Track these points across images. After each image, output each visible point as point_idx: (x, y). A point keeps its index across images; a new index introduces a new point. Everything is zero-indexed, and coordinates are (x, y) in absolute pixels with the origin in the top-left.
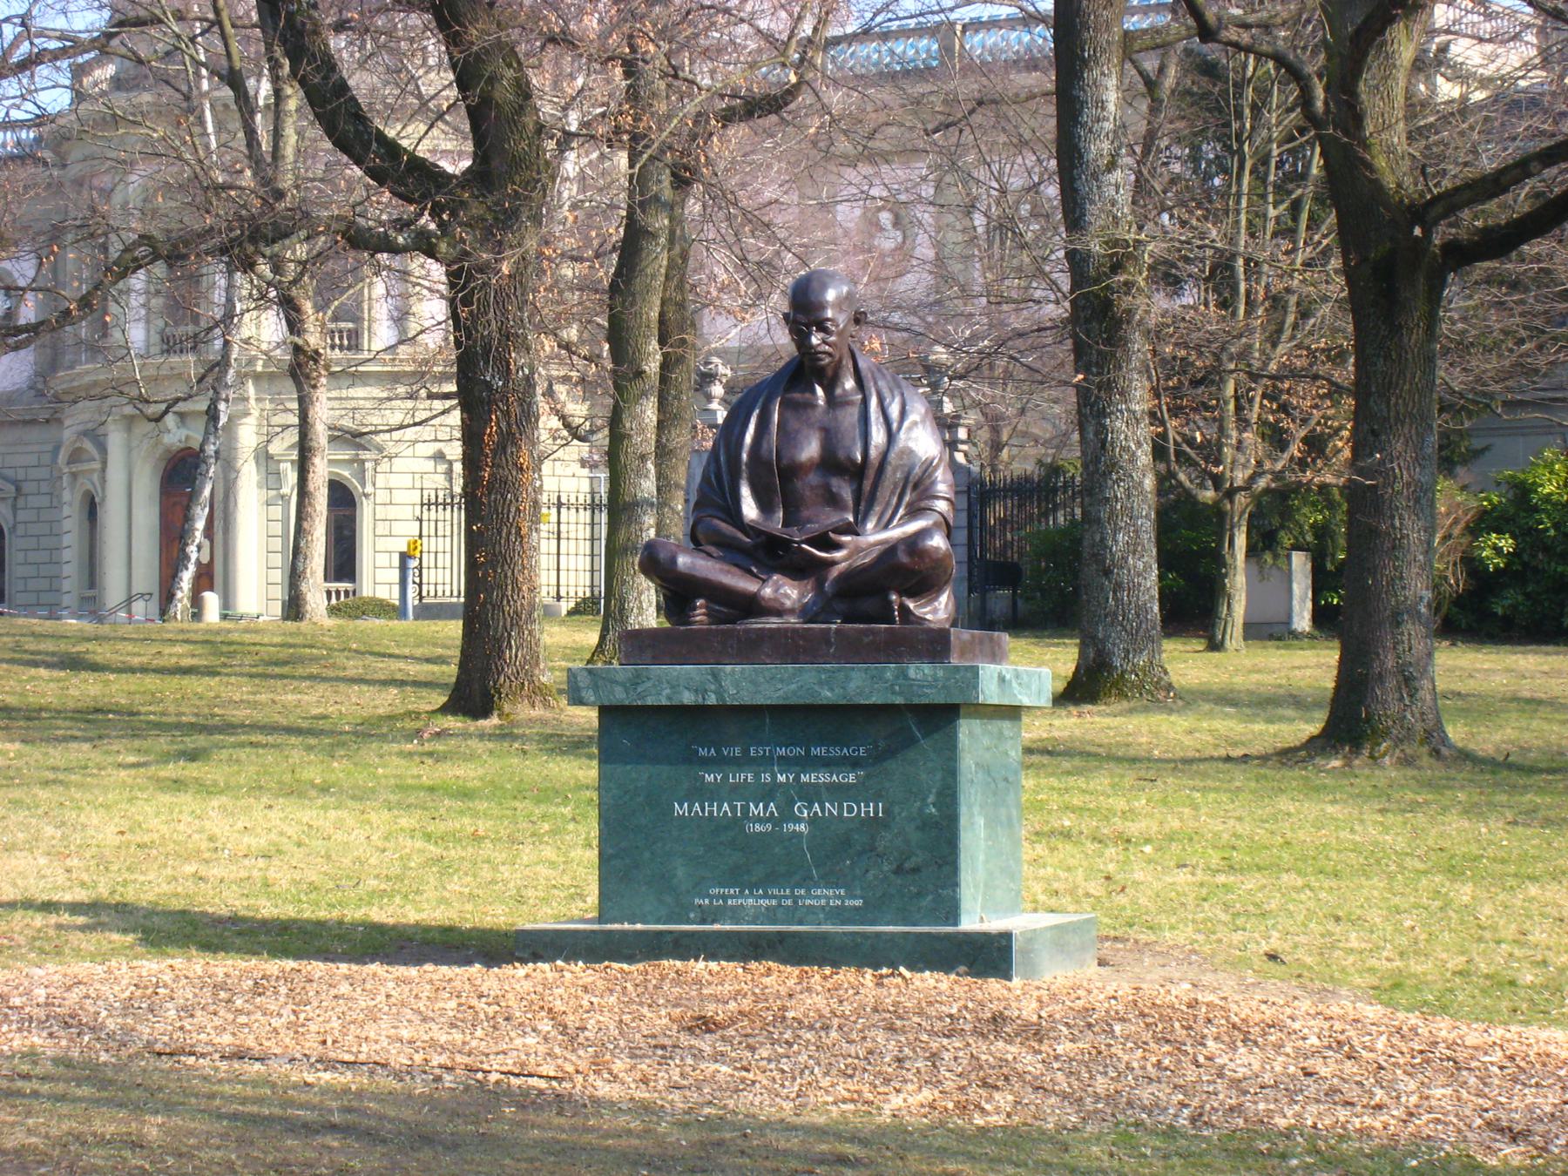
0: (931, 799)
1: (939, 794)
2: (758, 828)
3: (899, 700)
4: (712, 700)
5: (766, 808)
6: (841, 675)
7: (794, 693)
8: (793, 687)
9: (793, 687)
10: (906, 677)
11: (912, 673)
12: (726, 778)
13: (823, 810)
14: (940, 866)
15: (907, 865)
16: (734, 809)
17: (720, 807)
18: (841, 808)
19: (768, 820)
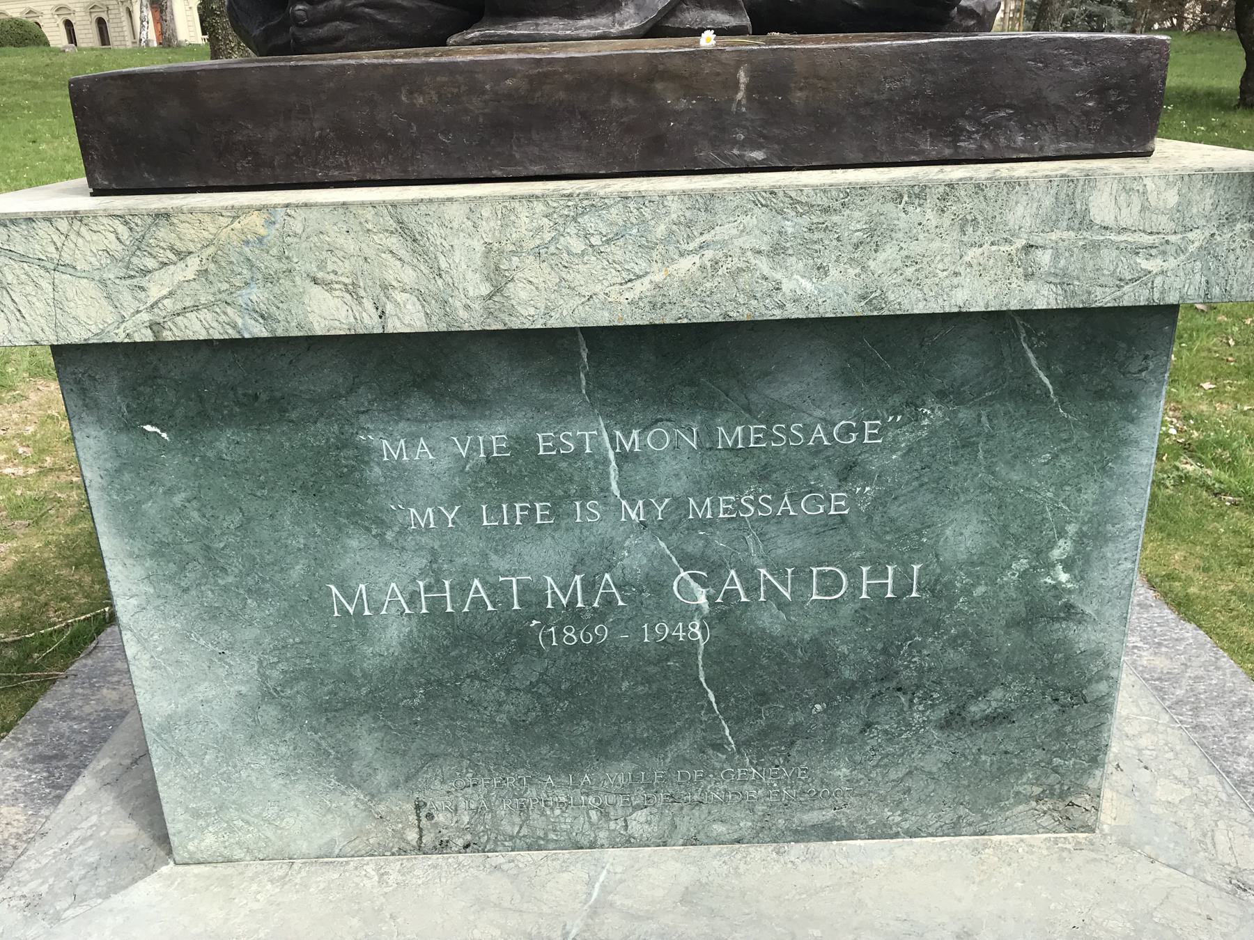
0: (1061, 549)
1: (1081, 538)
2: (571, 635)
3: (1043, 297)
4: (408, 317)
5: (590, 587)
6: (853, 222)
7: (690, 288)
8: (685, 265)
9: (685, 265)
10: (1083, 221)
11: (1102, 207)
12: (471, 514)
13: (751, 589)
14: (1064, 709)
15: (976, 709)
16: (496, 590)
17: (461, 589)
18: (801, 578)
19: (600, 616)
